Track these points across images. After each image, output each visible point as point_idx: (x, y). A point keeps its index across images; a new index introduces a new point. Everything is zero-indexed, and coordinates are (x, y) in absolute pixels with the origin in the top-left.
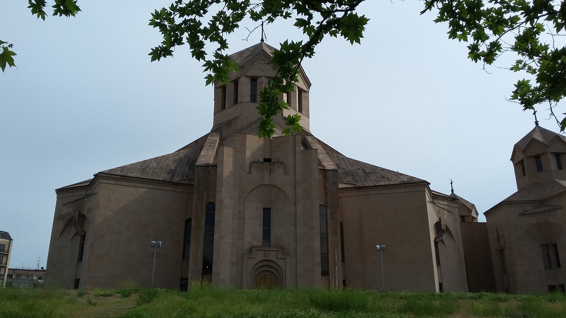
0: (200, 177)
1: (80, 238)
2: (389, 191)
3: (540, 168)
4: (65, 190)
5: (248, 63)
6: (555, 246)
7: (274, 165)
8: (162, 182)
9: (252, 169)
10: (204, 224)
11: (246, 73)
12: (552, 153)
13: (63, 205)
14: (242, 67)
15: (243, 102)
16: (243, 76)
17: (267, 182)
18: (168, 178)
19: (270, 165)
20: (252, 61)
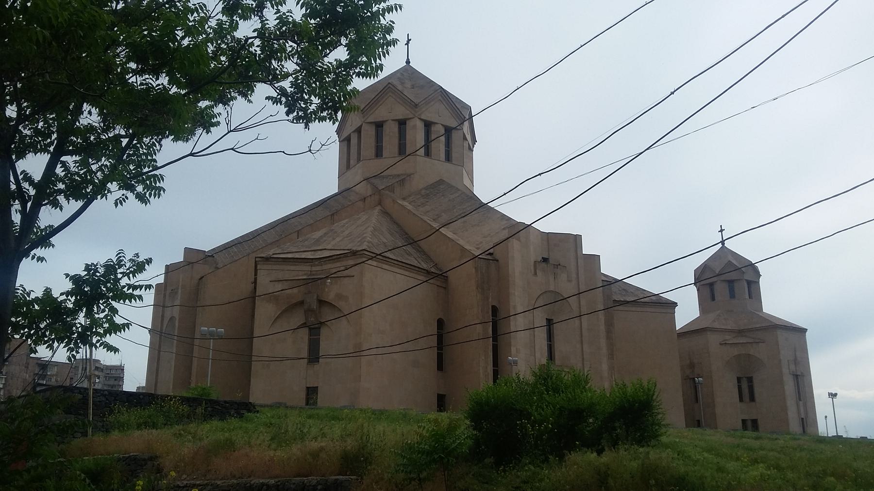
0: (484, 272)
1: (308, 331)
2: (639, 309)
3: (732, 295)
4: (273, 260)
5: (424, 102)
6: (750, 380)
7: (557, 268)
8: (417, 269)
9: (538, 271)
10: (491, 332)
11: (420, 115)
12: (747, 280)
13: (271, 281)
14: (416, 105)
15: (418, 155)
16: (418, 119)
17: (552, 288)
18: (415, 263)
19: (554, 268)
20: (429, 99)
